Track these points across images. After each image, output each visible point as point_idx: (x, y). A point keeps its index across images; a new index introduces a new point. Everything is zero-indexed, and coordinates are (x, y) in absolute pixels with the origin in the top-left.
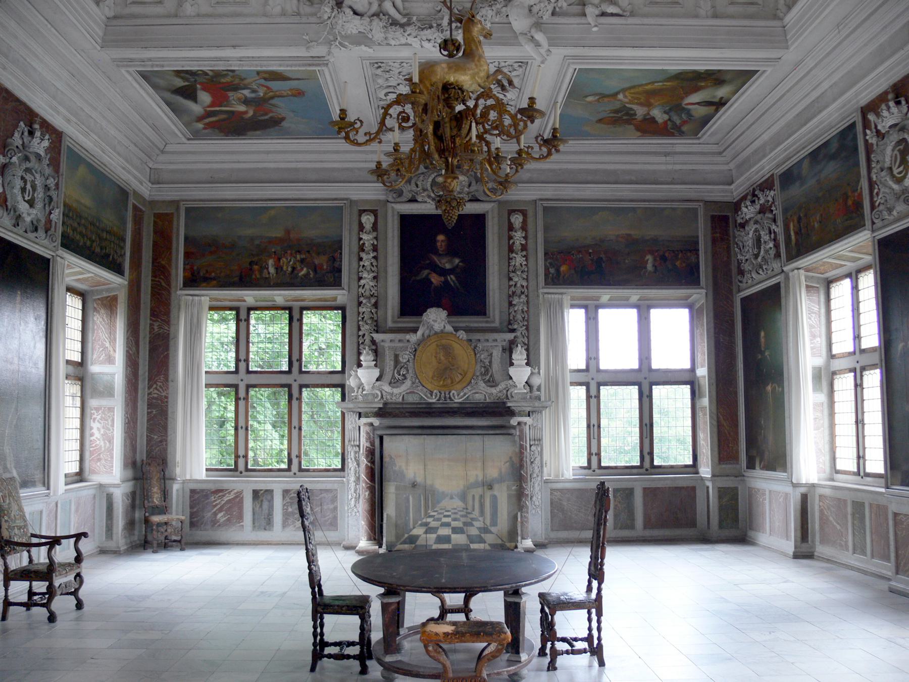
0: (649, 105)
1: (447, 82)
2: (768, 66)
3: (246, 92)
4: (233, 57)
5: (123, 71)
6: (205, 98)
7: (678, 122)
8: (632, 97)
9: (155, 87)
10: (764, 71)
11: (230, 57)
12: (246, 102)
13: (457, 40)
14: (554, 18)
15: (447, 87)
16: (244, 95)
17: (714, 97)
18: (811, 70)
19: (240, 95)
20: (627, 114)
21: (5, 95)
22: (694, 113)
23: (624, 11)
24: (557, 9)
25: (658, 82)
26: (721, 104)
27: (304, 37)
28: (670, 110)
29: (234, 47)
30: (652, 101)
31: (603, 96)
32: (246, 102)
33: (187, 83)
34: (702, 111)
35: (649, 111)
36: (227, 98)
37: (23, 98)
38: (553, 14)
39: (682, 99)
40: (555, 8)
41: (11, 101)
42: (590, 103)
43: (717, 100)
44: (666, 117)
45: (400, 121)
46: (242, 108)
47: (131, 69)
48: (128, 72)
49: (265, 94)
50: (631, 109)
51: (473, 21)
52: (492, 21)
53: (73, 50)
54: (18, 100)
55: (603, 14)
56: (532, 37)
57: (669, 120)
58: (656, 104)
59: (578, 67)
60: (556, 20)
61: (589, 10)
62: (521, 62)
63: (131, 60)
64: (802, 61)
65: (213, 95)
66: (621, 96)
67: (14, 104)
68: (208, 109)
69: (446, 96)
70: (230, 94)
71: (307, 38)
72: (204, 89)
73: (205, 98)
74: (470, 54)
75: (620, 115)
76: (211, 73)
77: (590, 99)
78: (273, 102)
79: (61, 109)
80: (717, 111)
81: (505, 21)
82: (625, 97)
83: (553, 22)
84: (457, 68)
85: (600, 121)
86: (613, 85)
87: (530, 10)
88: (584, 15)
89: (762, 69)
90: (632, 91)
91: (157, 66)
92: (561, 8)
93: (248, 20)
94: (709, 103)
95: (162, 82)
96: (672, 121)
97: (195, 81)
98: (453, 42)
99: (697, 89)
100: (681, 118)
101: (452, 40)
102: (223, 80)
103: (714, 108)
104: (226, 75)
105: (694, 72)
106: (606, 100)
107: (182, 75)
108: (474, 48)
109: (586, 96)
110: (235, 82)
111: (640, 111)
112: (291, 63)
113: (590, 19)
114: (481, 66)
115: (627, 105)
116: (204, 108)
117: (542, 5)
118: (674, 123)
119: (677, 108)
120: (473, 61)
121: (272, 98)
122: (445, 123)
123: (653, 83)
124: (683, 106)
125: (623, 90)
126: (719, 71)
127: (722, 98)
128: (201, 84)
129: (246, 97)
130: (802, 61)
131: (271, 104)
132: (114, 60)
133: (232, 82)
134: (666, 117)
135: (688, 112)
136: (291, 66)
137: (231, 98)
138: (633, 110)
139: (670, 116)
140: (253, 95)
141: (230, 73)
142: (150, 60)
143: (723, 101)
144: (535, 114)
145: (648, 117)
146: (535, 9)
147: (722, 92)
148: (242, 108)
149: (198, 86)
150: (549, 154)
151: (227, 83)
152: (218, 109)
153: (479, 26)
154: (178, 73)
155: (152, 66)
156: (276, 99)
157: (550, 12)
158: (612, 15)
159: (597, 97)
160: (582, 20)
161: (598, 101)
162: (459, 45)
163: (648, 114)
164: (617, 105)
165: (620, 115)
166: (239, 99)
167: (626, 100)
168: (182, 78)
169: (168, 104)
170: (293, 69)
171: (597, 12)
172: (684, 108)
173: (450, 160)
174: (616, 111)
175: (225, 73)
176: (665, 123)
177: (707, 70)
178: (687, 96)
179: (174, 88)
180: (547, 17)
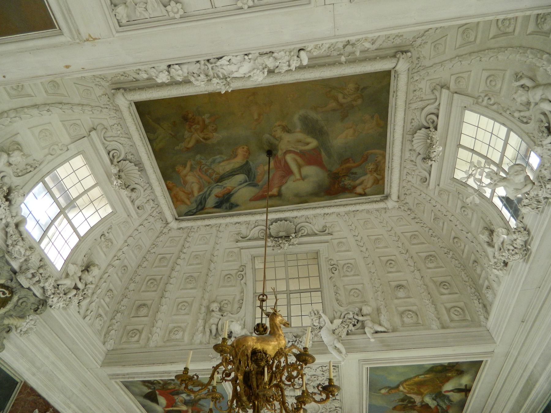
0: (420, 394)
1: (256, 348)
2: (488, 357)
3: (184, 396)
4: (173, 371)
5: (113, 381)
6: (162, 400)
7: (444, 407)
8: (409, 388)
9: (133, 393)
10: (487, 361)
11: (171, 371)
12: (186, 403)
13: (265, 324)
14: (348, 336)
15: (255, 352)
16: (184, 398)
17: (461, 385)
18: (516, 358)
19: (181, 398)
20: (410, 402)
21: (29, 391)
22: (452, 398)
23: (388, 330)
24: (349, 331)
25: (421, 375)
26: (467, 390)
27: (210, 356)
28: (436, 396)
29: (172, 363)
30: (422, 390)
31: (391, 389)
32: (186, 403)
33: (150, 390)
34: (456, 397)
35: (423, 398)
36: (174, 401)
37: (44, 395)
38: (348, 334)
39: (441, 387)
40: (348, 331)
41: (34, 395)
42: (384, 395)
43: (463, 387)
44: (435, 403)
45: (224, 376)
46: (184, 408)
47: (118, 380)
48: (116, 382)
49: (195, 397)
50: (411, 398)
51: (276, 314)
52: (313, 341)
53: (86, 369)
54: (39, 396)
55: (377, 332)
56: (336, 347)
57: (438, 405)
58: (425, 392)
59: (369, 366)
60: (349, 337)
61: (367, 330)
62: (335, 366)
63: (118, 375)
64: (508, 353)
65: (167, 399)
66: (401, 388)
67: (35, 397)
68: (167, 409)
69: (255, 358)
70: (176, 397)
71: (211, 356)
72: (160, 394)
73: (162, 400)
74: (274, 333)
75: (405, 403)
76: (162, 382)
77: (383, 391)
78: (201, 402)
79: (72, 406)
80: (467, 396)
81: (321, 340)
82: (404, 388)
83: (348, 339)
84: (264, 341)
85: (394, 408)
86: (394, 379)
87: (334, 333)
88: (365, 333)
89: (484, 359)
90: (407, 383)
91: (131, 378)
92: (351, 330)
93: (181, 348)
94: (459, 390)
95: (136, 390)
96: (440, 406)
97: (155, 388)
98: (263, 325)
99: (448, 379)
100: (445, 403)
101: (262, 324)
102: (170, 387)
103: (463, 394)
104: (170, 384)
105: (442, 365)
106: (393, 391)
107: (147, 384)
108: (276, 330)
109: (380, 390)
110: (176, 389)
111: (417, 399)
112: (203, 373)
113: (369, 335)
114: (281, 340)
115: (409, 395)
116: (163, 408)
117: (340, 329)
118: (442, 409)
119: (439, 396)
120: (275, 337)
121: (200, 399)
122: (253, 375)
123: (418, 376)
124: (443, 393)
125: (402, 383)
126: (457, 363)
127: (466, 386)
128: (158, 390)
129: (185, 400)
130: (508, 353)
131: (200, 404)
132: (109, 375)
133: (175, 388)
134: (435, 403)
135: (448, 398)
136: (204, 375)
137: (177, 400)
138: (412, 398)
139: (438, 402)
140: (188, 398)
141: (172, 382)
142: (128, 374)
143: (468, 388)
144: (307, 357)
145: (423, 404)
146: (337, 332)
147: (465, 380)
148: (184, 408)
149: (157, 392)
150: (328, 398)
151: (172, 389)
152: (171, 409)
153: (280, 318)
154: (145, 383)
155: (128, 378)
156: (202, 400)
157: (345, 333)
158: (381, 332)
159: (387, 390)
160: (364, 336)
161: (388, 392)
162: (266, 328)
163: (423, 401)
164: (402, 396)
165: (405, 403)
166: (181, 401)
167: (405, 391)
168: (147, 386)
169: (144, 406)
170: (205, 376)
171: (372, 331)
172: (444, 396)
173: (256, 403)
174: (403, 400)
175: (169, 381)
176: (436, 407)
177: (449, 363)
178: (443, 385)
179: (144, 394)
180: (344, 335)
